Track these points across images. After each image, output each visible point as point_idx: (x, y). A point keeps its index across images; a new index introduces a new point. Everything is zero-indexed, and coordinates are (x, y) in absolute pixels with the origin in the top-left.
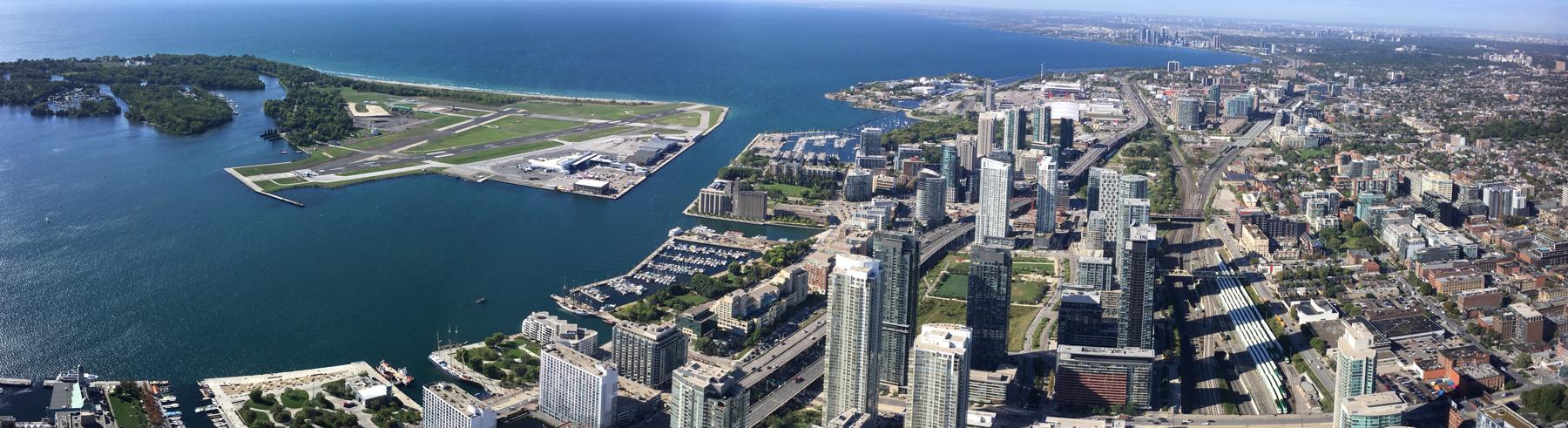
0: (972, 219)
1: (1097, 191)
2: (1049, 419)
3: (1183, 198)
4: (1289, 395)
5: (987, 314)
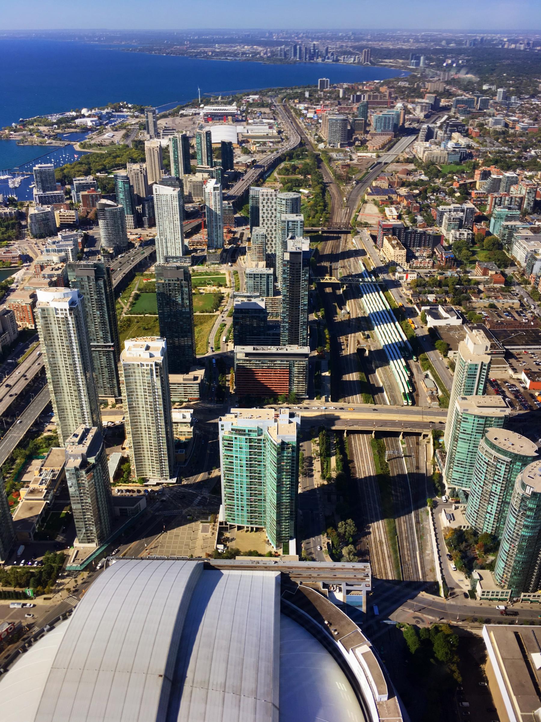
0: (152, 242)
1: (257, 209)
2: (233, 410)
3: (332, 213)
4: (414, 389)
5: (176, 324)
